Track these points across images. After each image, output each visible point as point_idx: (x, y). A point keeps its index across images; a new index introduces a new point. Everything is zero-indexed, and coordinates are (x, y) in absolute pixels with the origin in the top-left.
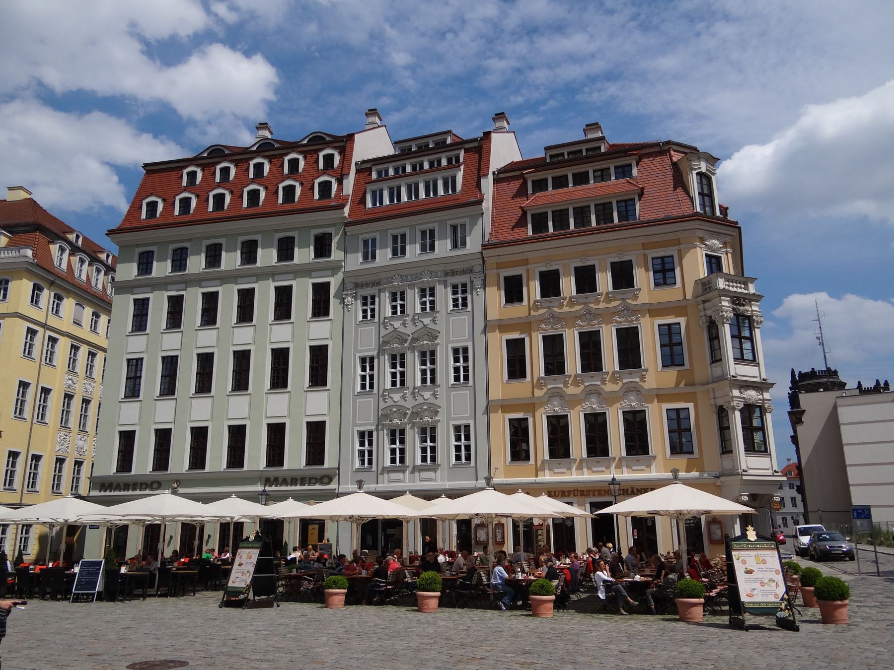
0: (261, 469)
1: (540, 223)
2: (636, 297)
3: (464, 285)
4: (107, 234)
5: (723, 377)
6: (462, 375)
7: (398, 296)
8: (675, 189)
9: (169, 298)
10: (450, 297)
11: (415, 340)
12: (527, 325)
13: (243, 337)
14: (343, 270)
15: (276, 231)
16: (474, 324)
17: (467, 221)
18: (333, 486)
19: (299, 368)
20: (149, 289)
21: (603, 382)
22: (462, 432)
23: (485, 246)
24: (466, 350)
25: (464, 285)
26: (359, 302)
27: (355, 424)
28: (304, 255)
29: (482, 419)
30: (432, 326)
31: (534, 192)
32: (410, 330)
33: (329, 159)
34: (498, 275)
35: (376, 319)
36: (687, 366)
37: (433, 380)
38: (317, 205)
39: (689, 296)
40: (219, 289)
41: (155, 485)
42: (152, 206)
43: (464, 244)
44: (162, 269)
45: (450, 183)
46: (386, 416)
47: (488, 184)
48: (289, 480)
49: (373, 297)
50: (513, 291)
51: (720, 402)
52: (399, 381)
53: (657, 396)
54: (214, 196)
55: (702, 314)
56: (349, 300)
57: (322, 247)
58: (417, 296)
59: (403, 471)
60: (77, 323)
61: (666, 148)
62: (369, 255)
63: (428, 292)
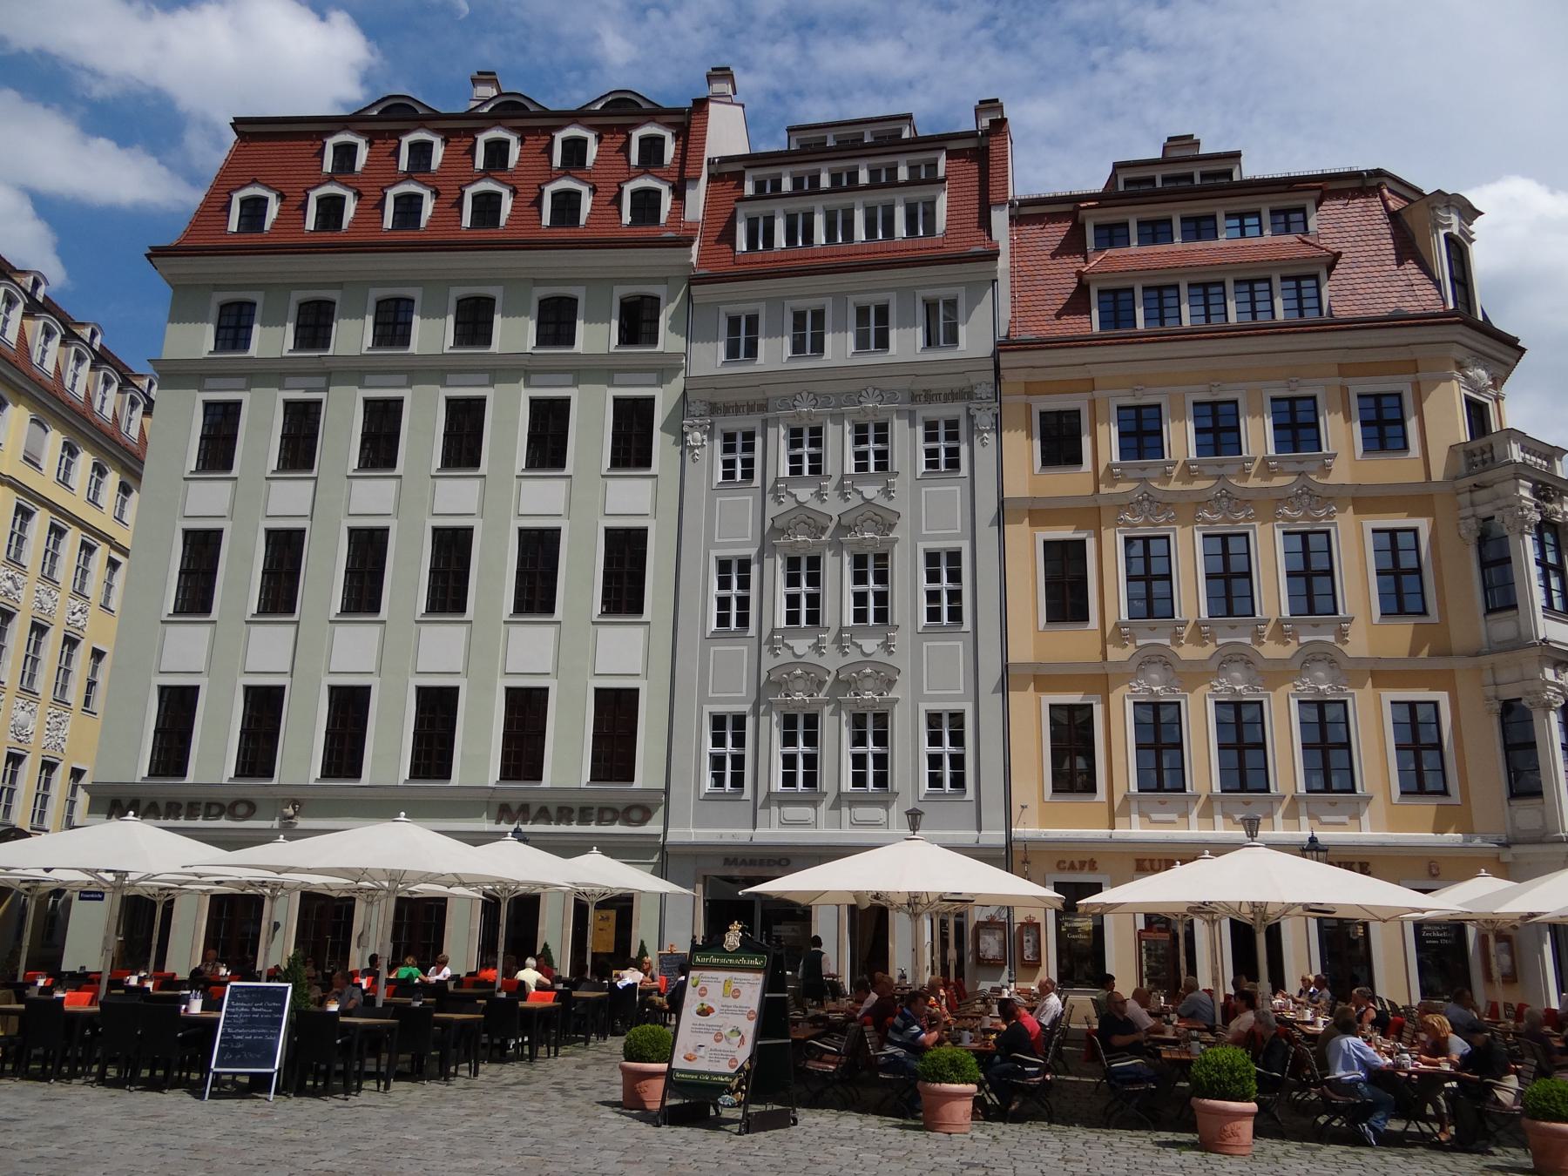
0: (491, 783)
1: (1117, 308)
2: (1326, 470)
3: (952, 425)
4: (149, 256)
5: (1523, 643)
6: (946, 609)
7: (807, 437)
8: (1400, 262)
9: (288, 405)
10: (922, 446)
12: (1092, 514)
14: (682, 373)
15: (537, 282)
16: (970, 505)
17: (961, 294)
18: (653, 827)
19: (581, 573)
20: (242, 382)
21: (1258, 637)
22: (946, 727)
23: (1005, 346)
24: (954, 557)
25: (952, 425)
26: (718, 444)
27: (704, 699)
28: (595, 336)
34: (1029, 407)
35: (757, 481)
36: (1434, 615)
37: (882, 616)
38: (628, 235)
39: (1438, 474)
40: (406, 394)
41: (241, 809)
42: (254, 208)
43: (953, 339)
44: (272, 340)
45: (920, 215)
46: (778, 685)
48: (553, 811)
49: (749, 436)
50: (1061, 442)
51: (1509, 693)
53: (1373, 674)
54: (397, 199)
55: (1468, 512)
56: (695, 437)
57: (637, 322)
58: (849, 439)
59: (814, 804)
60: (32, 461)
61: (1374, 182)
63: (872, 433)
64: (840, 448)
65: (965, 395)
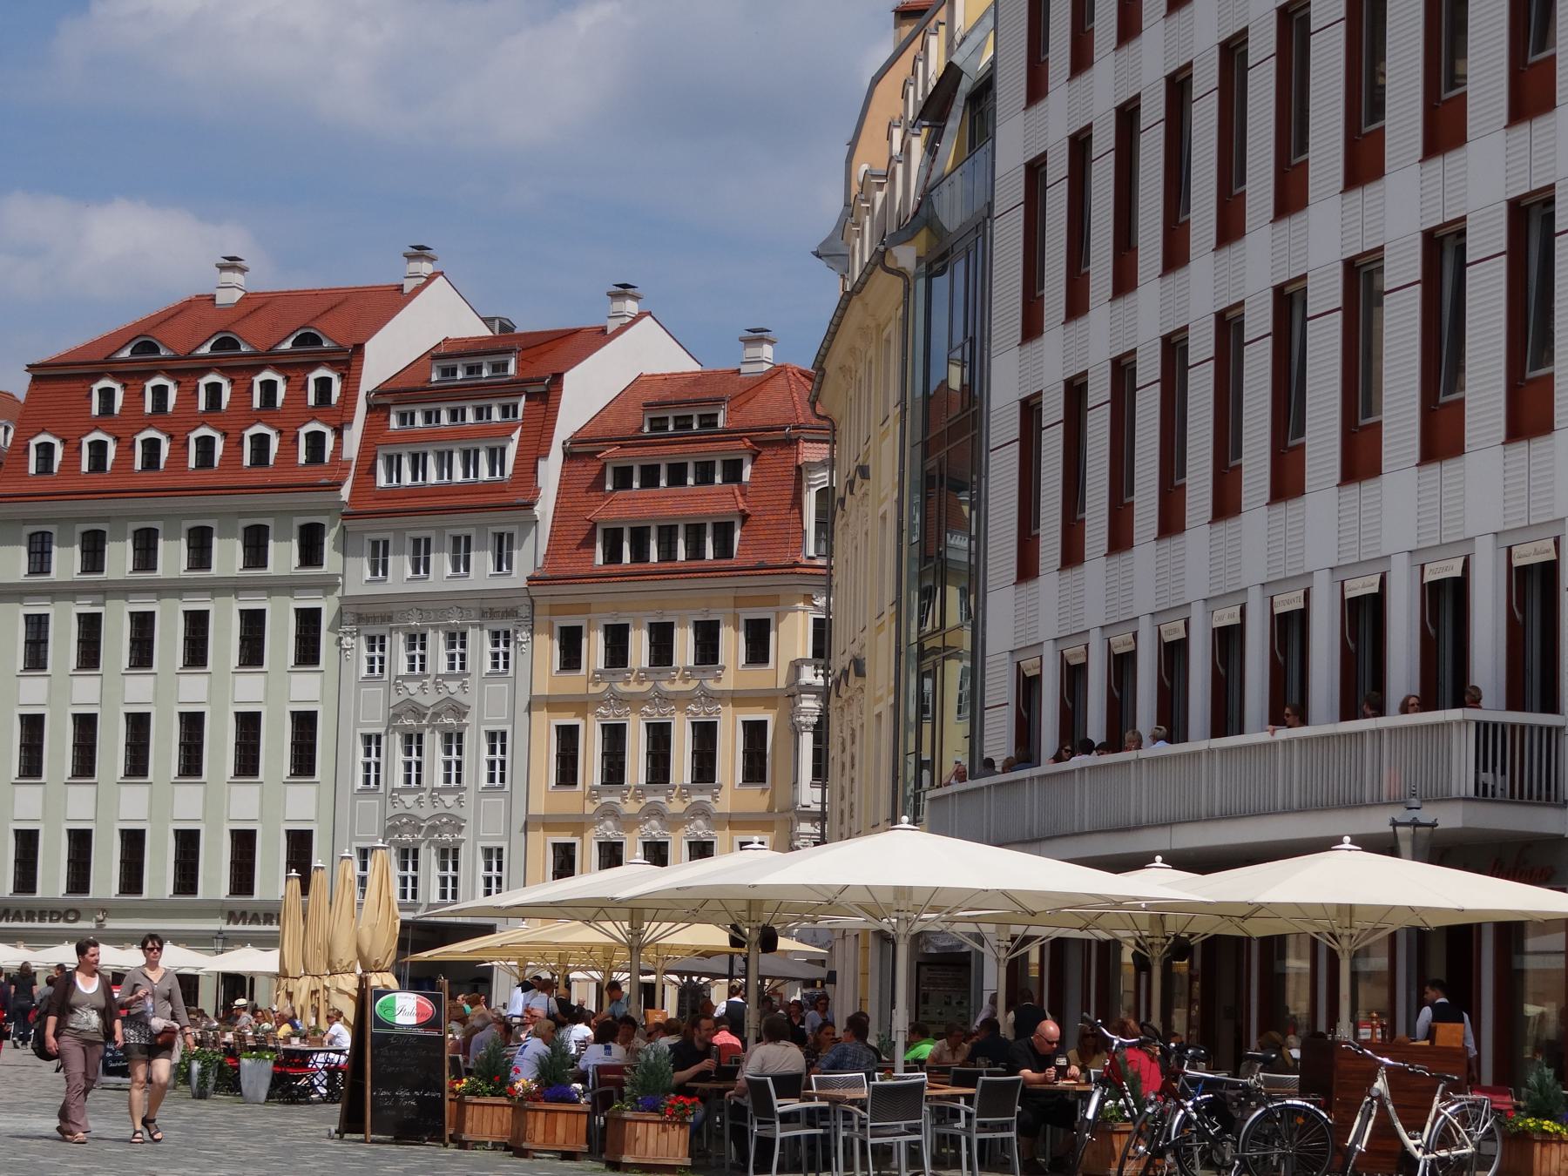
0: (223, 897)
2: (718, 679)
6: (498, 773)
7: (416, 640)
11: (436, 715)
12: (581, 705)
13: (193, 690)
14: (339, 593)
19: (276, 744)
29: (518, 837)
30: (460, 697)
31: (616, 488)
32: (428, 699)
33: (324, 385)
35: (386, 678)
38: (301, 478)
42: (46, 450)
44: (66, 562)
45: (497, 456)
46: (394, 829)
47: (551, 470)
52: (414, 773)
58: (442, 644)
62: (379, 565)
63: (456, 638)
64: (437, 647)
65: (510, 613)
